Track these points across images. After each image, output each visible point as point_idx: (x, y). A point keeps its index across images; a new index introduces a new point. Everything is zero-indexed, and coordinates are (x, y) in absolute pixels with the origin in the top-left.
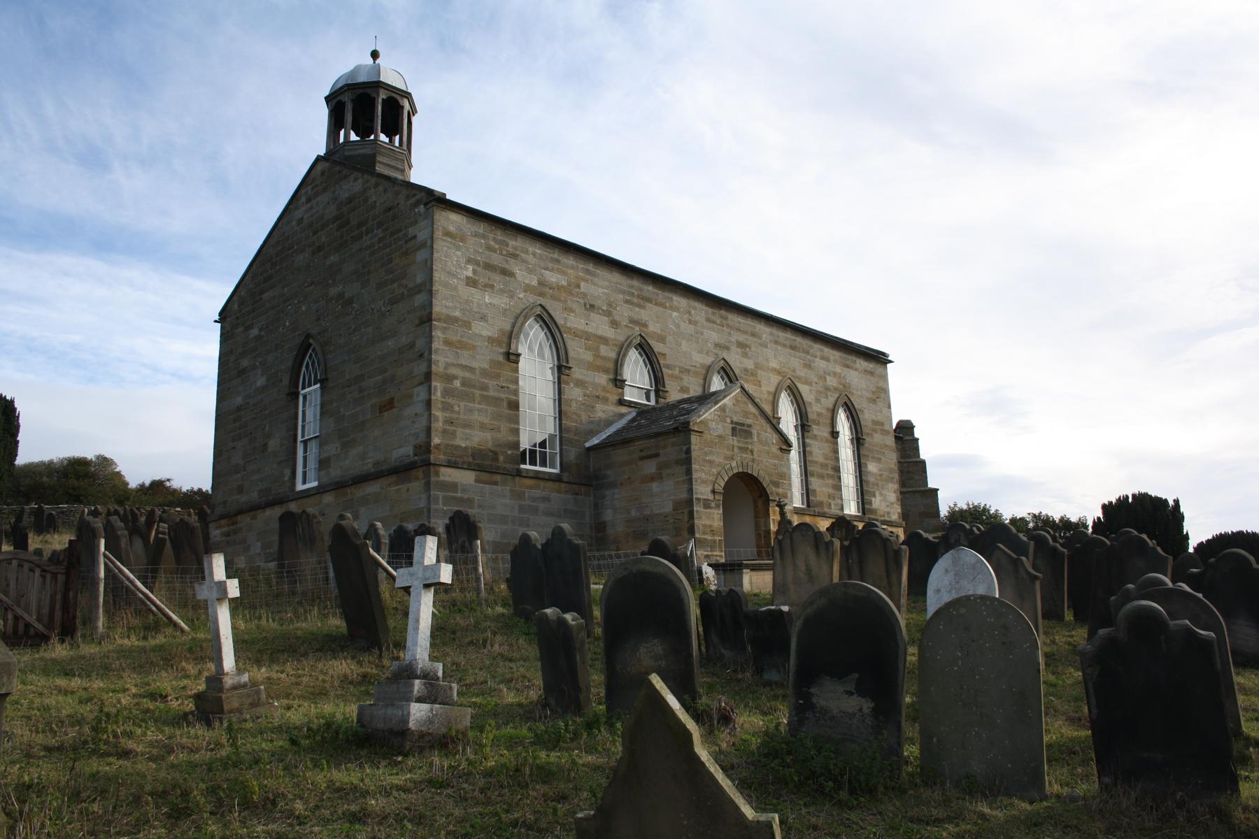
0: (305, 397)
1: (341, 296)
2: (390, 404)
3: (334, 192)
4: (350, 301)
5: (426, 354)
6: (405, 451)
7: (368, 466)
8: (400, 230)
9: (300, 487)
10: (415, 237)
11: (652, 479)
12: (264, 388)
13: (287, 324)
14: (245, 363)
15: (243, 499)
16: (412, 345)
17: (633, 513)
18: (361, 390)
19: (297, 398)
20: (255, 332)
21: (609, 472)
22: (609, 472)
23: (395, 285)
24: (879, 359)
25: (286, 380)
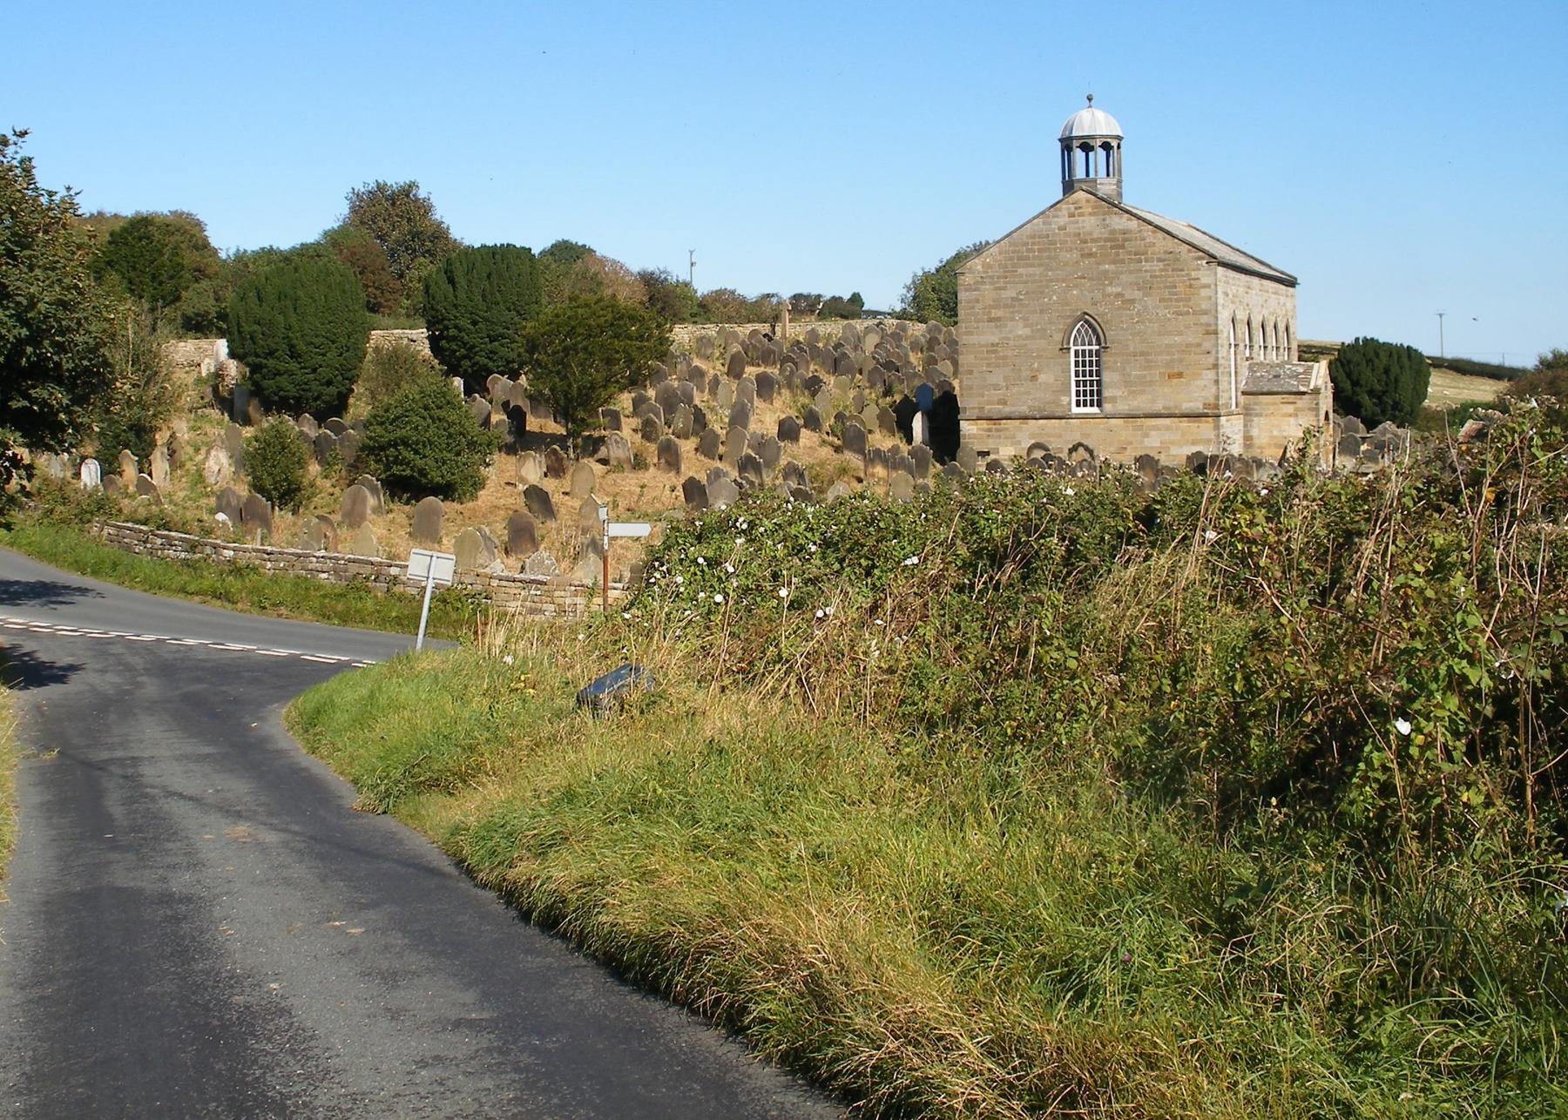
0: (1076, 352)
1: (1119, 295)
2: (1180, 375)
3: (1104, 220)
4: (1132, 301)
5: (1214, 352)
6: (1197, 406)
7: (1158, 407)
8: (1182, 270)
9: (1075, 410)
10: (1198, 279)
11: (1290, 416)
12: (1027, 338)
13: (1055, 298)
14: (995, 313)
15: (1007, 410)
16: (1199, 345)
17: (1275, 433)
18: (1148, 361)
19: (1069, 352)
20: (1011, 293)
21: (1255, 407)
22: (1255, 407)
23: (1181, 304)
24: (1291, 283)
25: (1058, 337)
